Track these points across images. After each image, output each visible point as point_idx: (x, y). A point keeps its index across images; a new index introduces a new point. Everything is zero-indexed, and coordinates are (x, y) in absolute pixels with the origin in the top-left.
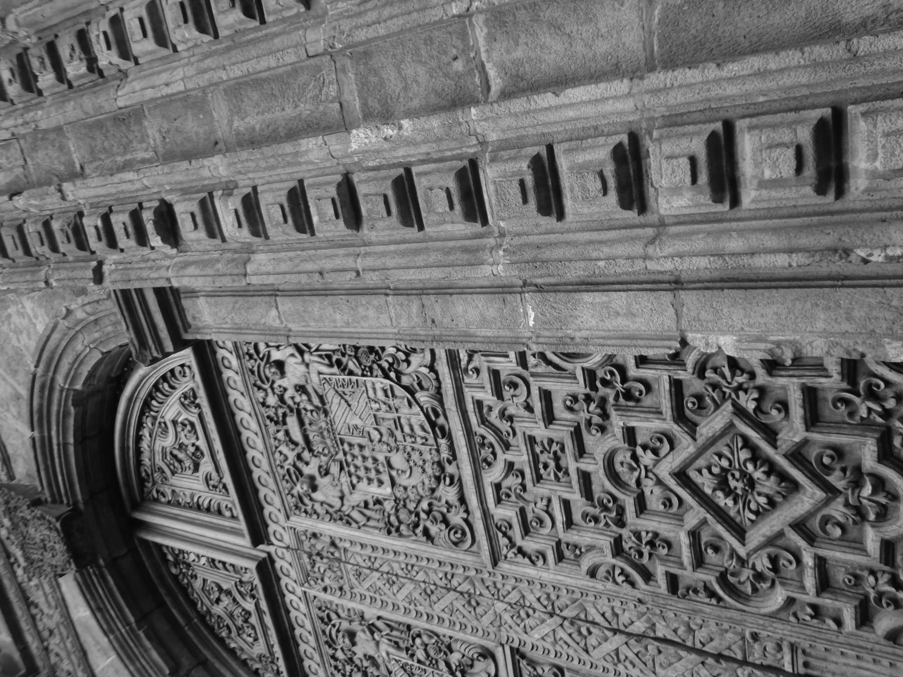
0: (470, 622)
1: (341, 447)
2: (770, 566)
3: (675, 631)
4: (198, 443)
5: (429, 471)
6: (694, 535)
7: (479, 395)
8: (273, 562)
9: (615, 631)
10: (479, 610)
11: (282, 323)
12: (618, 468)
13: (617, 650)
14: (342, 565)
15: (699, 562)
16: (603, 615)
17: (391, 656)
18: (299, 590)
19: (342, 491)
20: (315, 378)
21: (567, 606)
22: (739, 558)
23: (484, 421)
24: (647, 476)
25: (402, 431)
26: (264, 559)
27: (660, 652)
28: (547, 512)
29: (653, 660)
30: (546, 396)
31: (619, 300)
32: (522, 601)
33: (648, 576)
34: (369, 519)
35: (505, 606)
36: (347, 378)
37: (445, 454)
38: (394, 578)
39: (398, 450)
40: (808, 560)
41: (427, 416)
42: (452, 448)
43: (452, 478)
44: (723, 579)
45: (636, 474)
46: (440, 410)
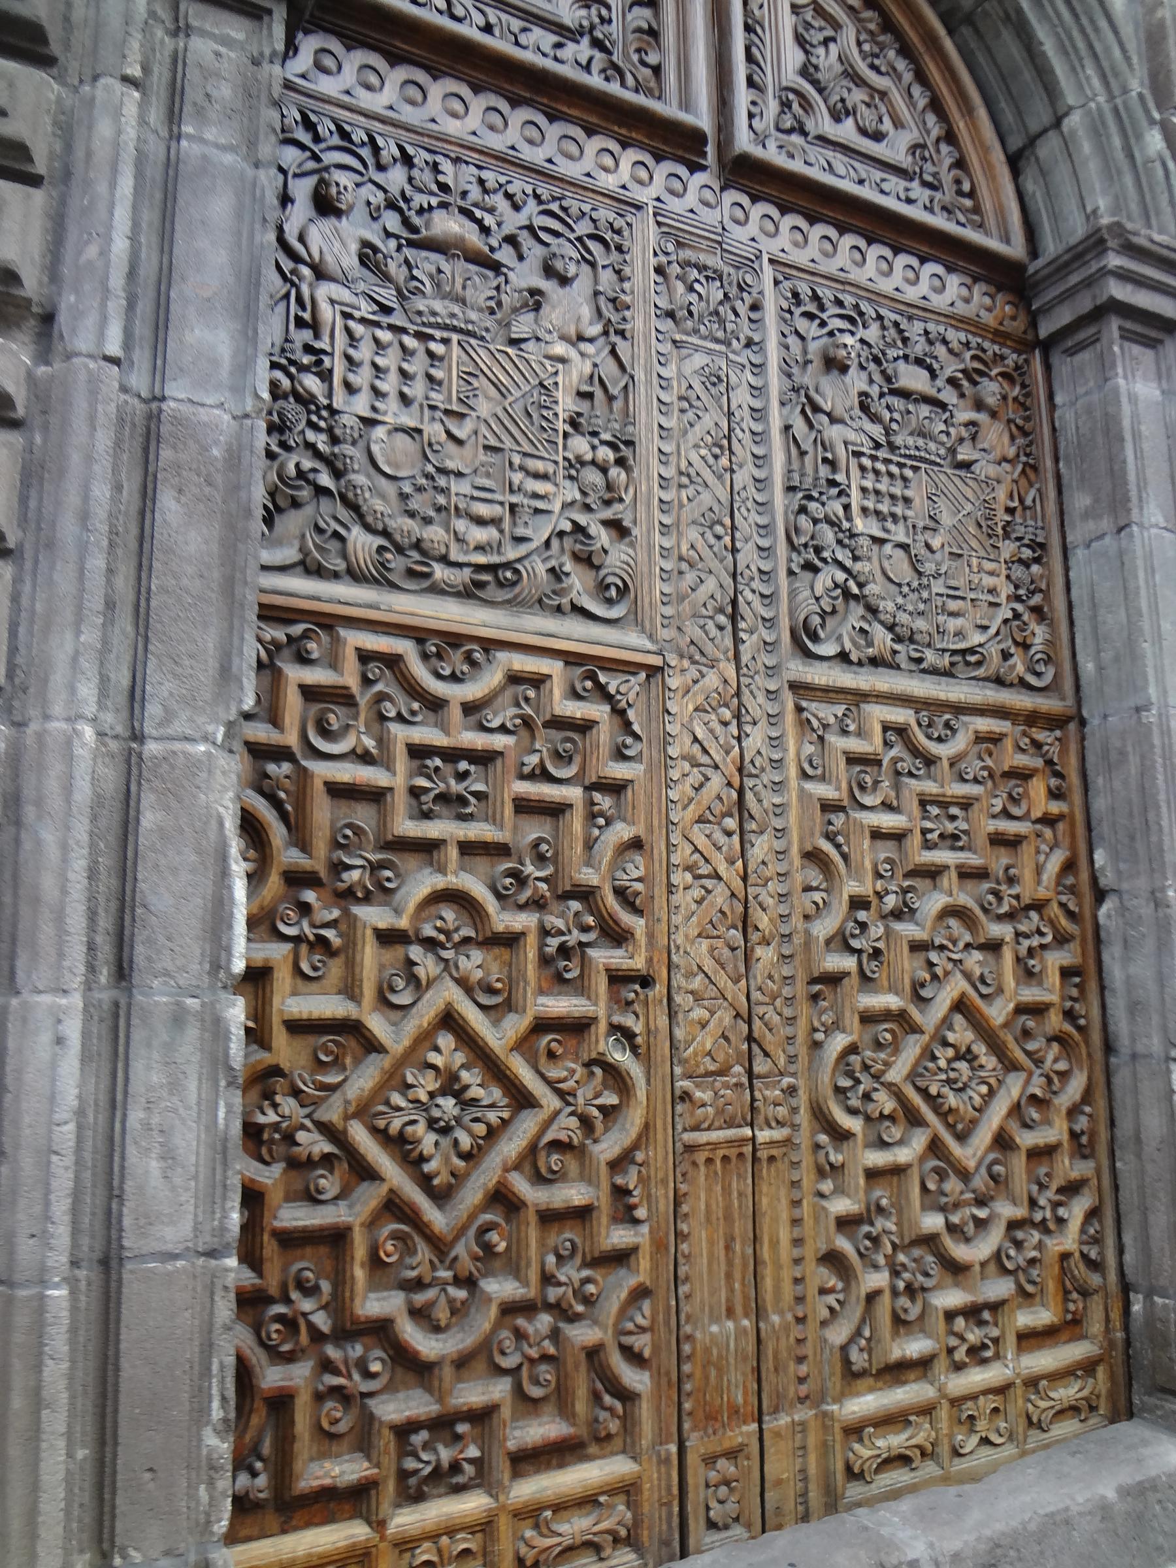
0: (682, 598)
1: (909, 462)
2: (886, 1112)
3: (770, 977)
4: (849, 122)
5: (903, 618)
6: (901, 1017)
7: (1008, 743)
8: (694, 168)
9: (745, 878)
10: (710, 625)
11: (1152, 526)
12: (953, 922)
13: (720, 878)
14: (723, 348)
15: (868, 1018)
16: (764, 863)
17: (560, 366)
18: (643, 195)
19: (841, 421)
20: (992, 470)
21: (760, 801)
22: (884, 1072)
24: (950, 959)
25: (948, 596)
26: (704, 155)
27: (733, 949)
28: (883, 803)
29: (719, 937)
32: (748, 719)
34: (803, 454)
35: (735, 685)
36: (1000, 531)
37: (930, 657)
38: (724, 461)
39: (920, 574)
40: (903, 1155)
41: (972, 651)
42: (934, 671)
43: (895, 652)
44: (852, 1049)
45: (950, 946)
46: (981, 672)
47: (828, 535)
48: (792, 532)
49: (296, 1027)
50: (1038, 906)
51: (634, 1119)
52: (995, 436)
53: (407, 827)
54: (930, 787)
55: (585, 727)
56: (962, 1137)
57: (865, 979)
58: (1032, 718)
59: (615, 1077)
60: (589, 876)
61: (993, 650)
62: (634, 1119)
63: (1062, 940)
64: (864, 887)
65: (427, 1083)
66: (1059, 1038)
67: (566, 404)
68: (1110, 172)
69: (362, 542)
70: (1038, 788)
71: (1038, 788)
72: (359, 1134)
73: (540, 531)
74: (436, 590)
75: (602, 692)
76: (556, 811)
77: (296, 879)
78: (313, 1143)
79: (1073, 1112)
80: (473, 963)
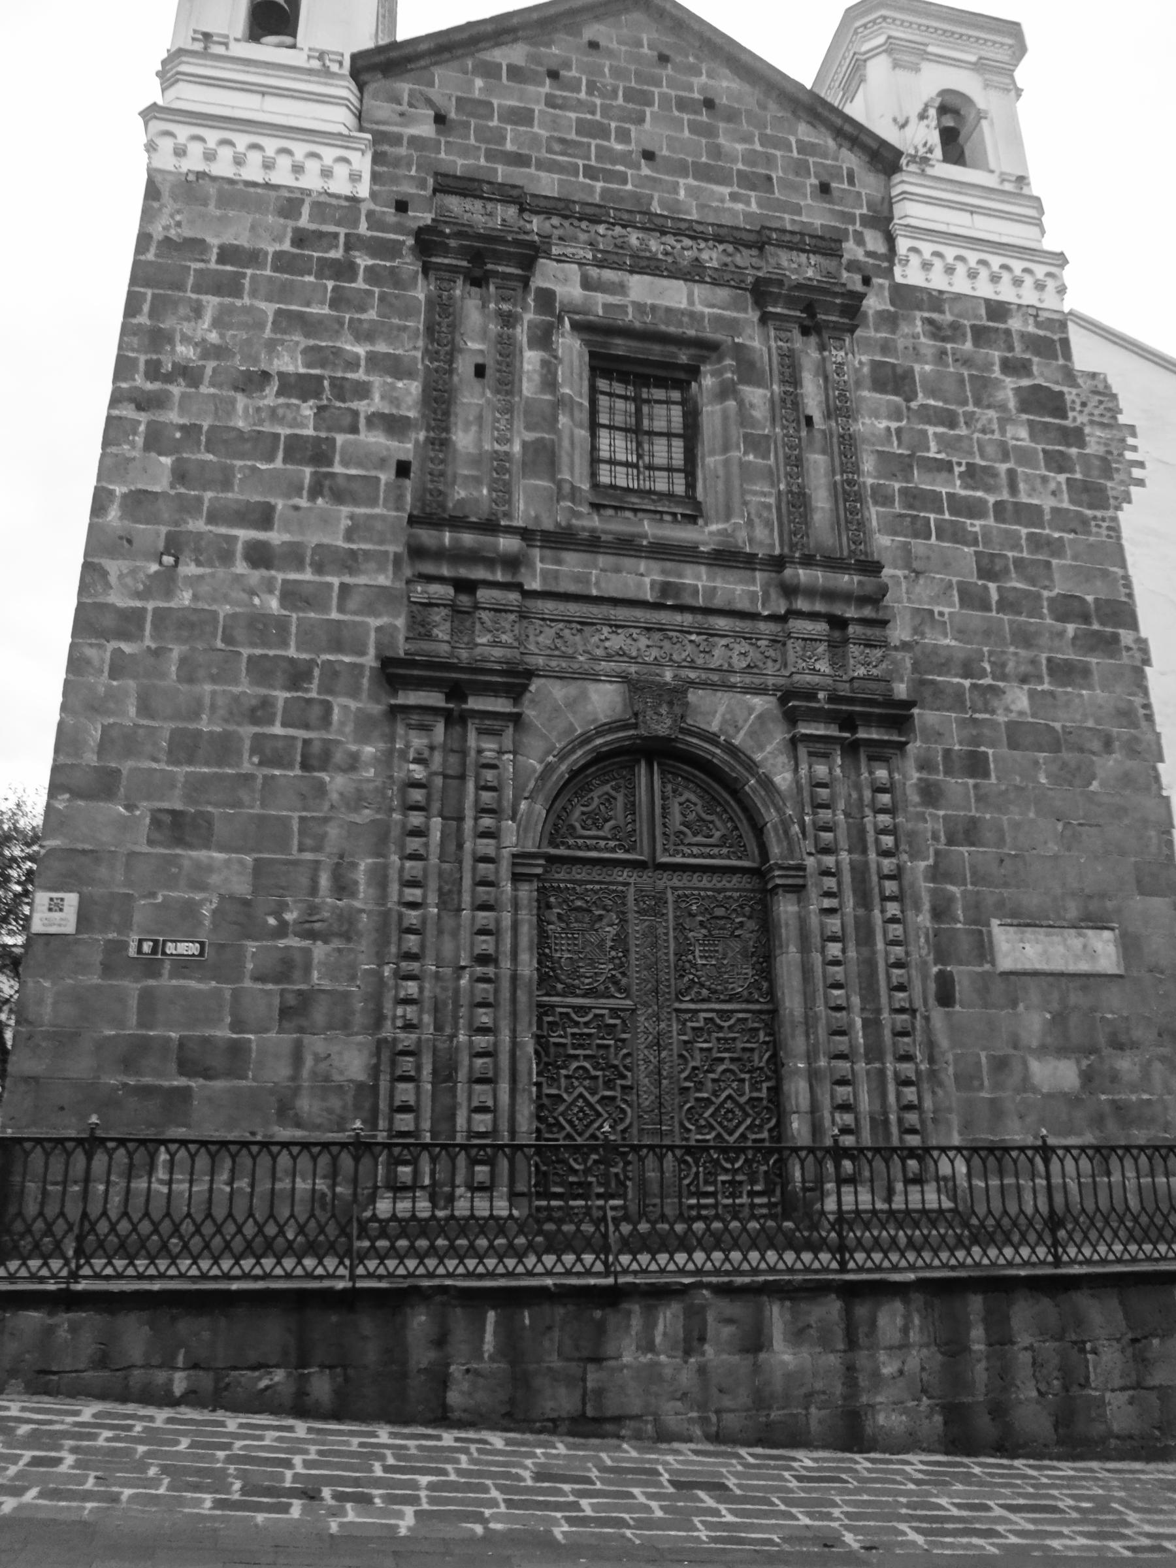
6: (708, 1099)
15: (697, 1099)
18: (632, 880)
23: (739, 1020)
30: (752, 1050)
31: (808, 1095)
33: (686, 1079)
47: (687, 965)
48: (676, 965)
49: (548, 1096)
50: (761, 1069)
51: (628, 1121)
52: (751, 925)
53: (572, 1052)
54: (721, 1035)
55: (615, 1026)
56: (731, 1134)
57: (699, 1090)
58: (760, 1012)
59: (623, 1111)
60: (616, 1062)
61: (745, 993)
62: (628, 1121)
63: (768, 1079)
64: (696, 1063)
65: (576, 1110)
66: (767, 1108)
67: (609, 944)
68: (779, 841)
69: (560, 986)
70: (762, 1034)
71: (762, 1034)
72: (561, 1119)
73: (602, 979)
74: (577, 996)
75: (619, 1017)
76: (607, 1047)
77: (547, 1064)
78: (551, 1120)
79: (770, 1130)
80: (587, 1083)
